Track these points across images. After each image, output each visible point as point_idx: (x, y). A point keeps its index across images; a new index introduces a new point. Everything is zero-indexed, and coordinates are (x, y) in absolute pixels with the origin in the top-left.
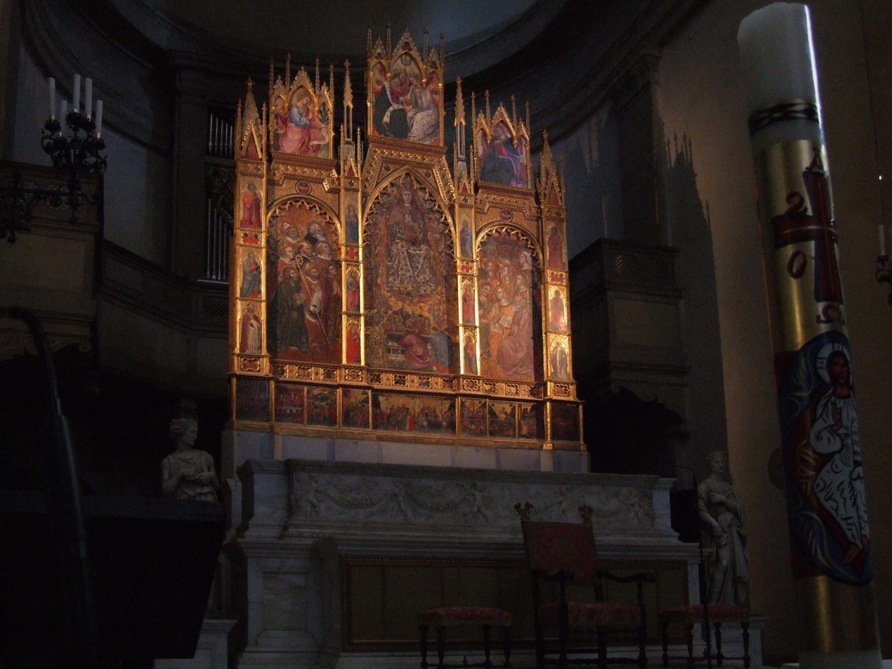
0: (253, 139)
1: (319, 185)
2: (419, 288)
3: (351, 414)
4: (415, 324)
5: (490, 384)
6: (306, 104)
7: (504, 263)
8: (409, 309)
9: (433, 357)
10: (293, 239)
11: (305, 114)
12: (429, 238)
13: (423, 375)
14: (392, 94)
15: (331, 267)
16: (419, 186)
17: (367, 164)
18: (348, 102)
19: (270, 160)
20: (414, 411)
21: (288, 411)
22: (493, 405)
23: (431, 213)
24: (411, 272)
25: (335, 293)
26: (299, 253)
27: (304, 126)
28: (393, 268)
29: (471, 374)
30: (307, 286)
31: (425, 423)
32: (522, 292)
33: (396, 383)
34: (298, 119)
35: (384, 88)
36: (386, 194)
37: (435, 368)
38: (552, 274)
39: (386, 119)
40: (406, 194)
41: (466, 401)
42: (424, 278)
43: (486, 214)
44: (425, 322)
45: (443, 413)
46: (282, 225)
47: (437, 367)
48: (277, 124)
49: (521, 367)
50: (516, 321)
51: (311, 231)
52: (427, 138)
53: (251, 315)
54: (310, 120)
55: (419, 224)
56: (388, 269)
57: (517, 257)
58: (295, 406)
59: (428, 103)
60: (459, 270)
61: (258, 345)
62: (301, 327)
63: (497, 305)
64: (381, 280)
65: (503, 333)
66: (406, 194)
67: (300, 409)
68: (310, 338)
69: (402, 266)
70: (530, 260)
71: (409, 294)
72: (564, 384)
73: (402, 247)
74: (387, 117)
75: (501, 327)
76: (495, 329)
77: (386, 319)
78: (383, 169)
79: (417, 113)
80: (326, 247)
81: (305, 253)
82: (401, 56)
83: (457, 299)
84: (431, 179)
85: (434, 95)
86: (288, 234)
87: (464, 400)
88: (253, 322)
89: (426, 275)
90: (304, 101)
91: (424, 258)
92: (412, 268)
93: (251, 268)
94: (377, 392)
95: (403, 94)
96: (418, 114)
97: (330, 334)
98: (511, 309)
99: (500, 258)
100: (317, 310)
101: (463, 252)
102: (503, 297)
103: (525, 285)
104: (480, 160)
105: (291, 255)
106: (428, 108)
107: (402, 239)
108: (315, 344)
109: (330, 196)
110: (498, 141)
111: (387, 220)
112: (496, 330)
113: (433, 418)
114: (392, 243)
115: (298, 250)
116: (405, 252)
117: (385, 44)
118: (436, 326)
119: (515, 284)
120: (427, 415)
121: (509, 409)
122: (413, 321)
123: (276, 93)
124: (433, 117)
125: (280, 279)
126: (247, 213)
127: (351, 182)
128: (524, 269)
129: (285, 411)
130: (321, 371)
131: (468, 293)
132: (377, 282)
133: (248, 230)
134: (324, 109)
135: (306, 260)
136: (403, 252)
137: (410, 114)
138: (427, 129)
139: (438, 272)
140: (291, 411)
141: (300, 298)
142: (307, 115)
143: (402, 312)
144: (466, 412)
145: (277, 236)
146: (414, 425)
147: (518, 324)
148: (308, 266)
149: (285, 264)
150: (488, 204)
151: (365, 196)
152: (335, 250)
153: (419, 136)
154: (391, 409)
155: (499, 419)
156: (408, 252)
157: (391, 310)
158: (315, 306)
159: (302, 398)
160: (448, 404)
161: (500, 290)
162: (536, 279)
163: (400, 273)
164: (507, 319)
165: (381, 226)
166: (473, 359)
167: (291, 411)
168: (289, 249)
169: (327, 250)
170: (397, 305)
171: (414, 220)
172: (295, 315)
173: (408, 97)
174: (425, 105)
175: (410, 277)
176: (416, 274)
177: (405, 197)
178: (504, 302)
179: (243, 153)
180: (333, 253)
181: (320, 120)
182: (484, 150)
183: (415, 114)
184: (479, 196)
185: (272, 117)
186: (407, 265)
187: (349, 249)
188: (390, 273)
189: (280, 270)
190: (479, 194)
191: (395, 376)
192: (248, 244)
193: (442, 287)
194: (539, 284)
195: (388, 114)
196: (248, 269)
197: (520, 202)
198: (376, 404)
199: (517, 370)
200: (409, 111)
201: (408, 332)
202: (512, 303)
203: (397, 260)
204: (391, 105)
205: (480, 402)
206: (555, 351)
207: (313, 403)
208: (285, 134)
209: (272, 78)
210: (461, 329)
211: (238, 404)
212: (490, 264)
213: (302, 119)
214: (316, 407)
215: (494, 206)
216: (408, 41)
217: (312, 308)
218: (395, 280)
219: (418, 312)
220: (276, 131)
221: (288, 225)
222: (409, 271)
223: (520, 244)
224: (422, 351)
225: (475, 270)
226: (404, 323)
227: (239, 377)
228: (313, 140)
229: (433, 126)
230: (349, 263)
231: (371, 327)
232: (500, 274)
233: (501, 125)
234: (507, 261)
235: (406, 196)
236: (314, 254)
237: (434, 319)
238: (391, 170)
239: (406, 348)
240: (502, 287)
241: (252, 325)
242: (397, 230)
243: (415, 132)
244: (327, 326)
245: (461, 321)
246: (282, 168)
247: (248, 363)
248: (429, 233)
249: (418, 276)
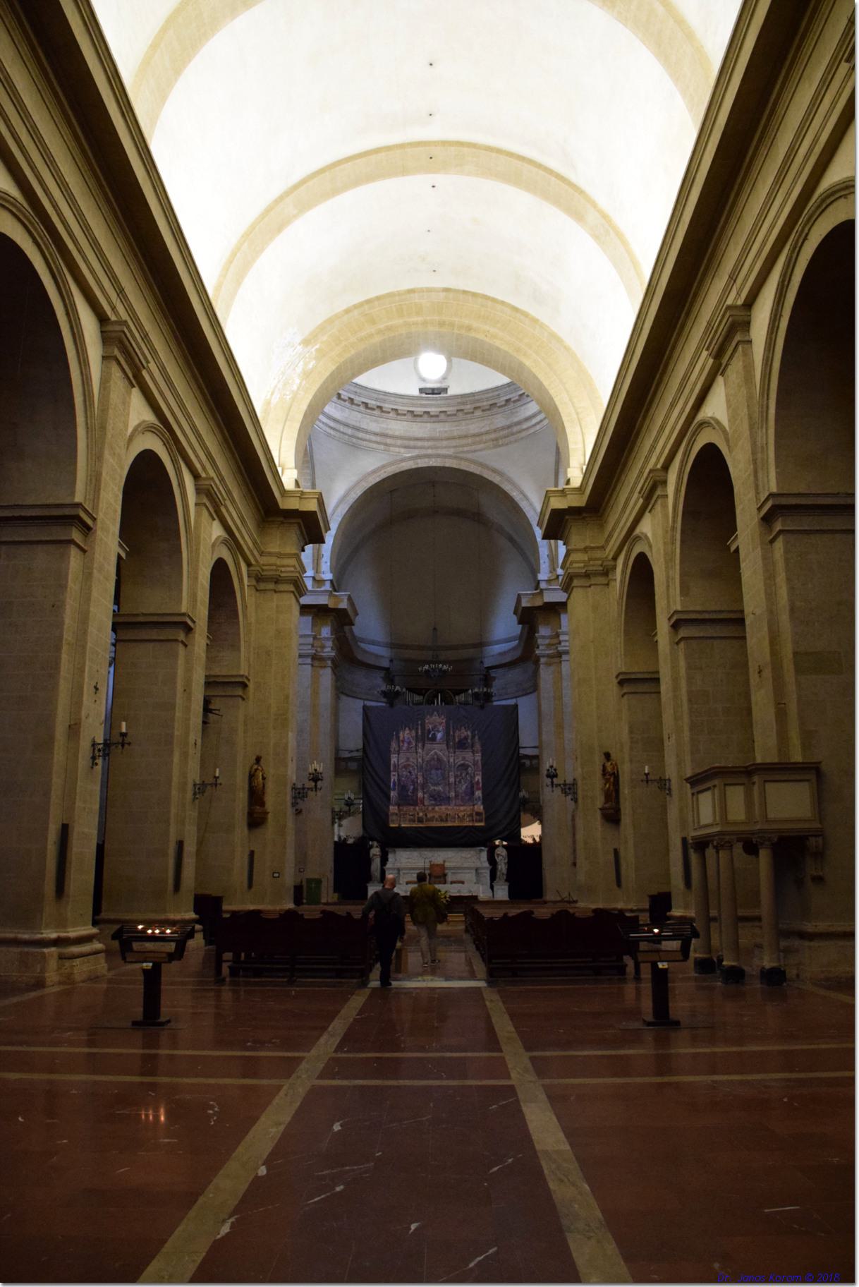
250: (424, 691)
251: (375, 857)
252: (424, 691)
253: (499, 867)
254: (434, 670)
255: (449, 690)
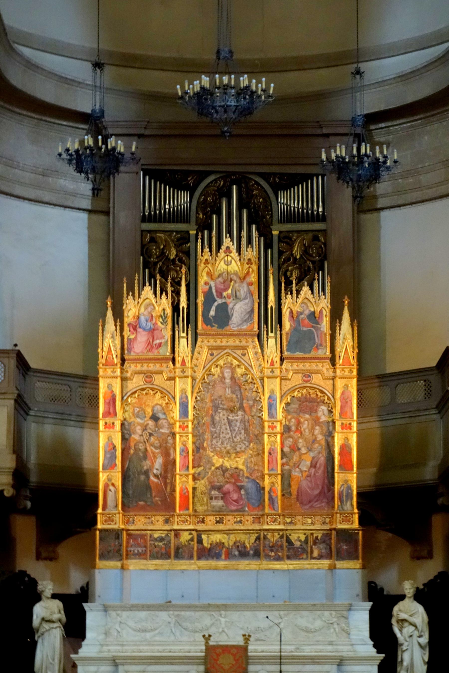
0: (111, 349)
1: (159, 375)
2: (236, 446)
3: (181, 550)
4: (232, 476)
5: (290, 518)
6: (151, 311)
7: (304, 418)
8: (227, 464)
9: (246, 500)
10: (141, 419)
11: (150, 319)
12: (245, 405)
13: (237, 515)
14: (217, 291)
15: (169, 438)
16: (237, 363)
17: (196, 353)
18: (183, 303)
19: (123, 361)
20: (229, 545)
21: (136, 551)
22: (290, 535)
23: (246, 384)
24: (230, 434)
25: (172, 457)
26: (146, 429)
27: (149, 329)
28: (216, 433)
29: (274, 512)
30: (151, 454)
31: (237, 553)
32: (319, 441)
33: (216, 523)
34: (145, 325)
35: (210, 288)
36: (210, 374)
37: (247, 509)
38: (342, 424)
39: (212, 313)
40: (227, 372)
41: (267, 534)
42: (240, 438)
43: (289, 380)
44: (239, 473)
45: (251, 544)
46: (134, 410)
47: (249, 508)
48: (130, 331)
49: (316, 502)
50: (313, 465)
51: (155, 412)
52: (245, 323)
53: (110, 483)
54: (154, 325)
55: (237, 395)
56: (212, 433)
57: (316, 411)
58: (141, 547)
59: (245, 294)
60: (266, 430)
61: (114, 504)
62: (148, 487)
63: (297, 453)
64: (207, 444)
65: (302, 475)
66: (227, 372)
67: (144, 549)
68: (154, 494)
69: (223, 430)
70: (326, 412)
71: (228, 452)
72: (348, 514)
73: (224, 415)
74: (213, 311)
75: (301, 471)
76: (296, 473)
77: (210, 474)
78: (209, 355)
79: (236, 303)
80: (166, 422)
81: (150, 429)
82: (224, 258)
83: (264, 453)
84: (246, 358)
85: (250, 287)
86: (138, 416)
87: (266, 534)
88: (111, 488)
89: (241, 435)
90: (149, 309)
91: (240, 422)
92: (231, 431)
93: (110, 448)
94: (199, 533)
95: (226, 289)
96: (237, 304)
97: (168, 489)
98: (309, 455)
99: (301, 415)
100: (159, 472)
101: (271, 415)
102: (303, 446)
103: (321, 434)
104: (287, 334)
105: (140, 432)
106: (245, 298)
107: (223, 409)
108: (157, 499)
109: (168, 382)
110: (303, 316)
111: (212, 395)
112: (296, 474)
113: (243, 549)
114: (215, 413)
115: (145, 428)
116: (226, 418)
117: (211, 251)
118: (248, 475)
119: (313, 434)
120: (238, 546)
121: (303, 538)
122: (230, 473)
123: (129, 307)
124: (249, 305)
125: (132, 452)
126: (107, 406)
127: (183, 370)
128: (321, 420)
129: (134, 551)
130: (161, 519)
131: (273, 447)
132: (203, 445)
133: (109, 420)
134: (164, 313)
135: (151, 435)
136: (224, 419)
137: (230, 306)
138: (244, 316)
139: (251, 432)
140: (138, 551)
141: (146, 464)
142: (152, 320)
143: (222, 468)
144: (267, 543)
145: (130, 418)
146: (229, 556)
147: (315, 467)
148: (152, 439)
149: (135, 440)
150: (291, 371)
151: (194, 379)
152: (173, 424)
153: (237, 322)
154: (211, 544)
155: (295, 546)
156: (227, 418)
157: (214, 466)
158: (157, 469)
159: (145, 541)
160: (255, 537)
161: (300, 441)
162: (331, 428)
163: (221, 436)
164: (306, 464)
165: (207, 400)
166: (276, 500)
167: (138, 551)
168: (139, 427)
169: (166, 425)
170: (218, 461)
171: (233, 392)
172: (143, 477)
173: (230, 291)
174: (242, 297)
175: (230, 438)
176: (234, 435)
177: (226, 375)
178: (304, 450)
179: (103, 361)
180: (171, 426)
181: (161, 323)
182: (291, 325)
183: (234, 305)
184: (284, 366)
185: (126, 326)
186: (226, 429)
187: (181, 423)
188: (214, 437)
189: (132, 444)
190: (284, 364)
191: (216, 518)
192: (107, 429)
193: (254, 444)
194: (333, 432)
195: (213, 308)
196: (108, 449)
197: (320, 365)
198: (200, 541)
199: (313, 504)
200: (231, 302)
201: (227, 482)
202: (310, 450)
203: (219, 426)
204: (215, 301)
205: (279, 534)
206: (342, 488)
207: (154, 544)
208: (135, 338)
209: (125, 295)
210: (266, 477)
211: (100, 550)
212: (293, 420)
213: (148, 324)
214: (155, 547)
215: (296, 372)
216: (229, 245)
217: (155, 471)
218: (217, 442)
219: (233, 466)
220: (129, 336)
221: (138, 409)
222: (228, 434)
223: (319, 400)
224: (237, 496)
225: (279, 428)
226: (224, 475)
227: (101, 531)
228: (156, 340)
229: (249, 312)
230: (181, 434)
231: (198, 481)
232: (301, 428)
233: (306, 301)
234: (307, 416)
235: (227, 374)
236: (157, 429)
237: (247, 471)
238: (215, 355)
239: (225, 496)
240: (303, 438)
241: (110, 490)
242: (220, 402)
243: (235, 319)
244: (166, 484)
245: (266, 471)
246: (133, 366)
247: (108, 519)
248: (245, 401)
249: (235, 437)
250: (191, 180)
251: (46, 626)
252: (191, 180)
253: (406, 657)
254: (226, 88)
255: (265, 176)
